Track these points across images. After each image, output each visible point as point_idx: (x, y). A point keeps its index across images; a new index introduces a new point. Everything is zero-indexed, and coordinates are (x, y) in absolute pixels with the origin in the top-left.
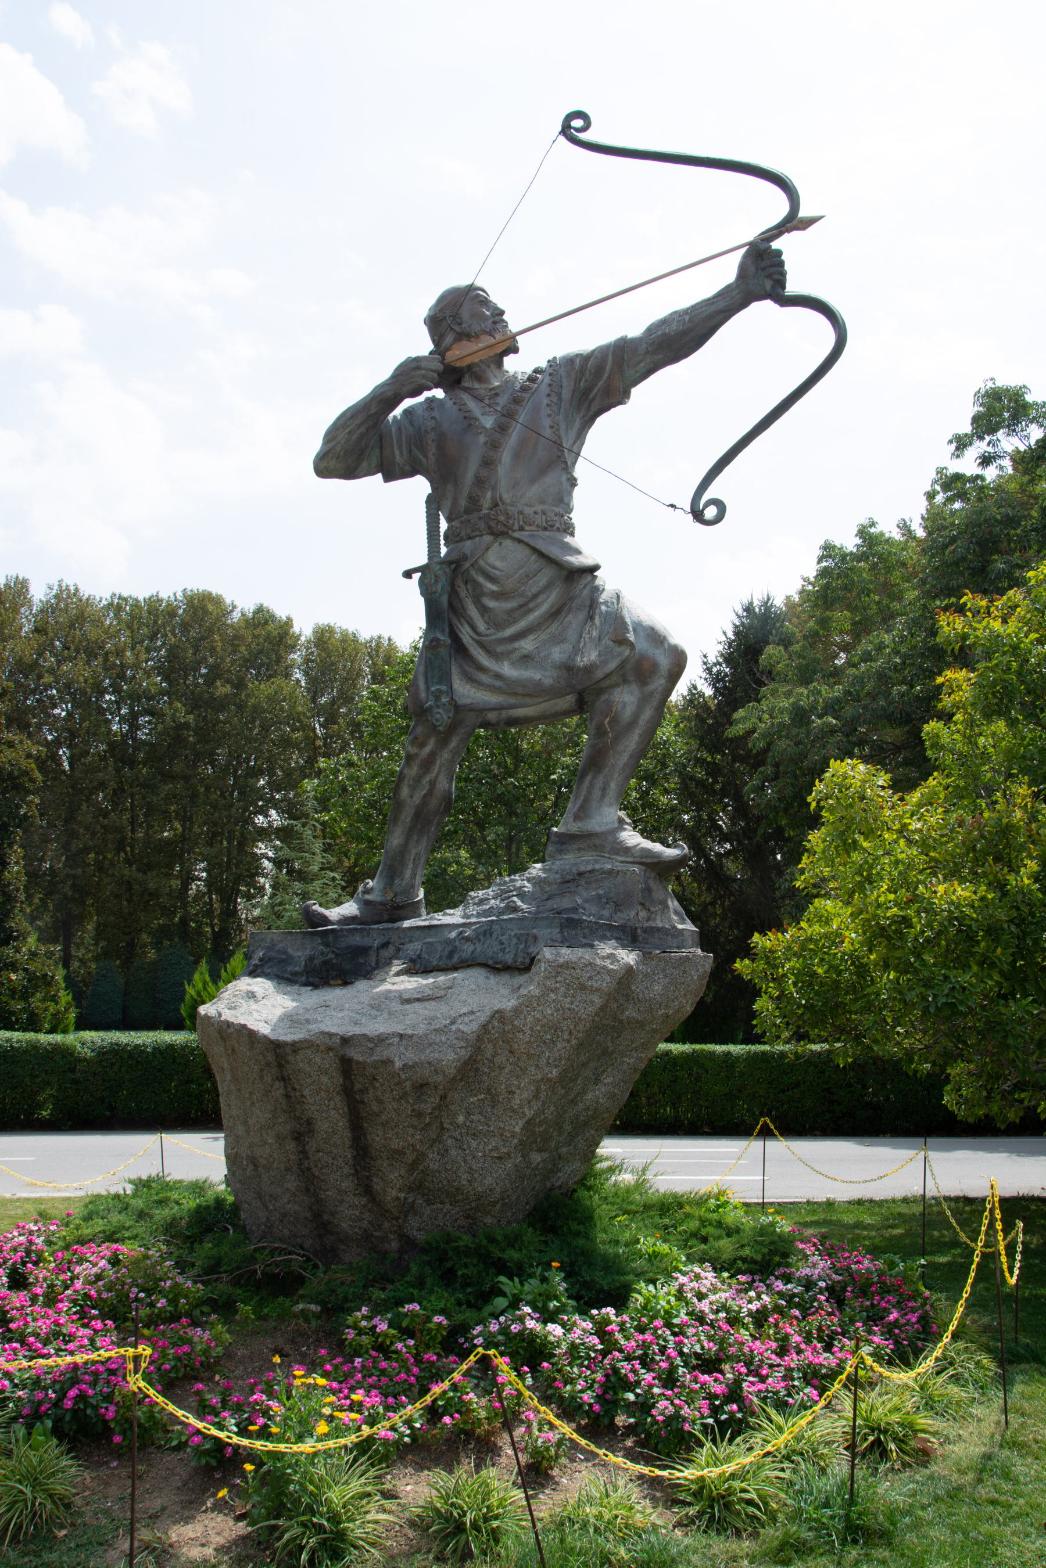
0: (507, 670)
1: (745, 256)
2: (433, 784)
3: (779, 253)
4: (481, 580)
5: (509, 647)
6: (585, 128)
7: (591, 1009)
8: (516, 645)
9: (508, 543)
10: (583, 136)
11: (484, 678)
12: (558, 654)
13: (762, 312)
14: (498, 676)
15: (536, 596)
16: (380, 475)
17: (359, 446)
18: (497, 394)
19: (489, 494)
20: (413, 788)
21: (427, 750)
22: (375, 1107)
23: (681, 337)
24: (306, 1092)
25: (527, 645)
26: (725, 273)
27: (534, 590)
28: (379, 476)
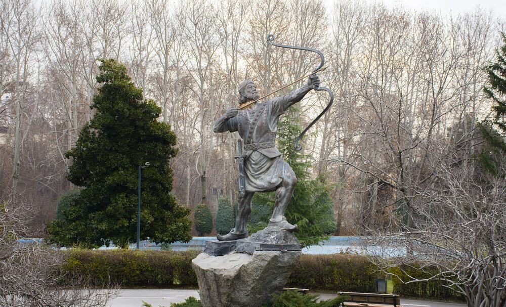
2: (245, 207)
7: (265, 265)
14: (255, 184)
15: (263, 164)
25: (263, 176)
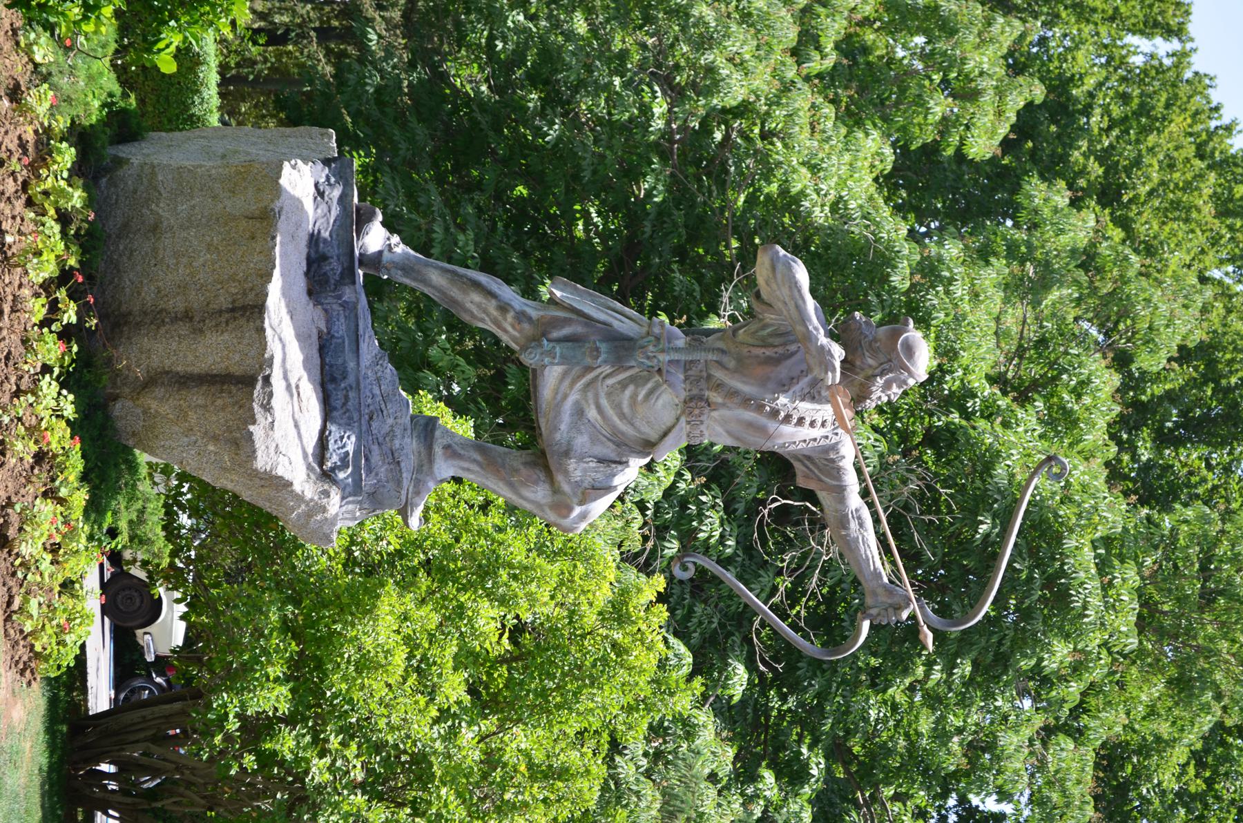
0: (574, 397)
2: (482, 320)
4: (649, 385)
5: (591, 401)
8: (593, 407)
11: (567, 383)
12: (581, 442)
14: (565, 396)
19: (720, 400)
20: (479, 306)
21: (510, 329)
22: (219, 402)
24: (226, 336)
25: (592, 413)
27: (638, 424)
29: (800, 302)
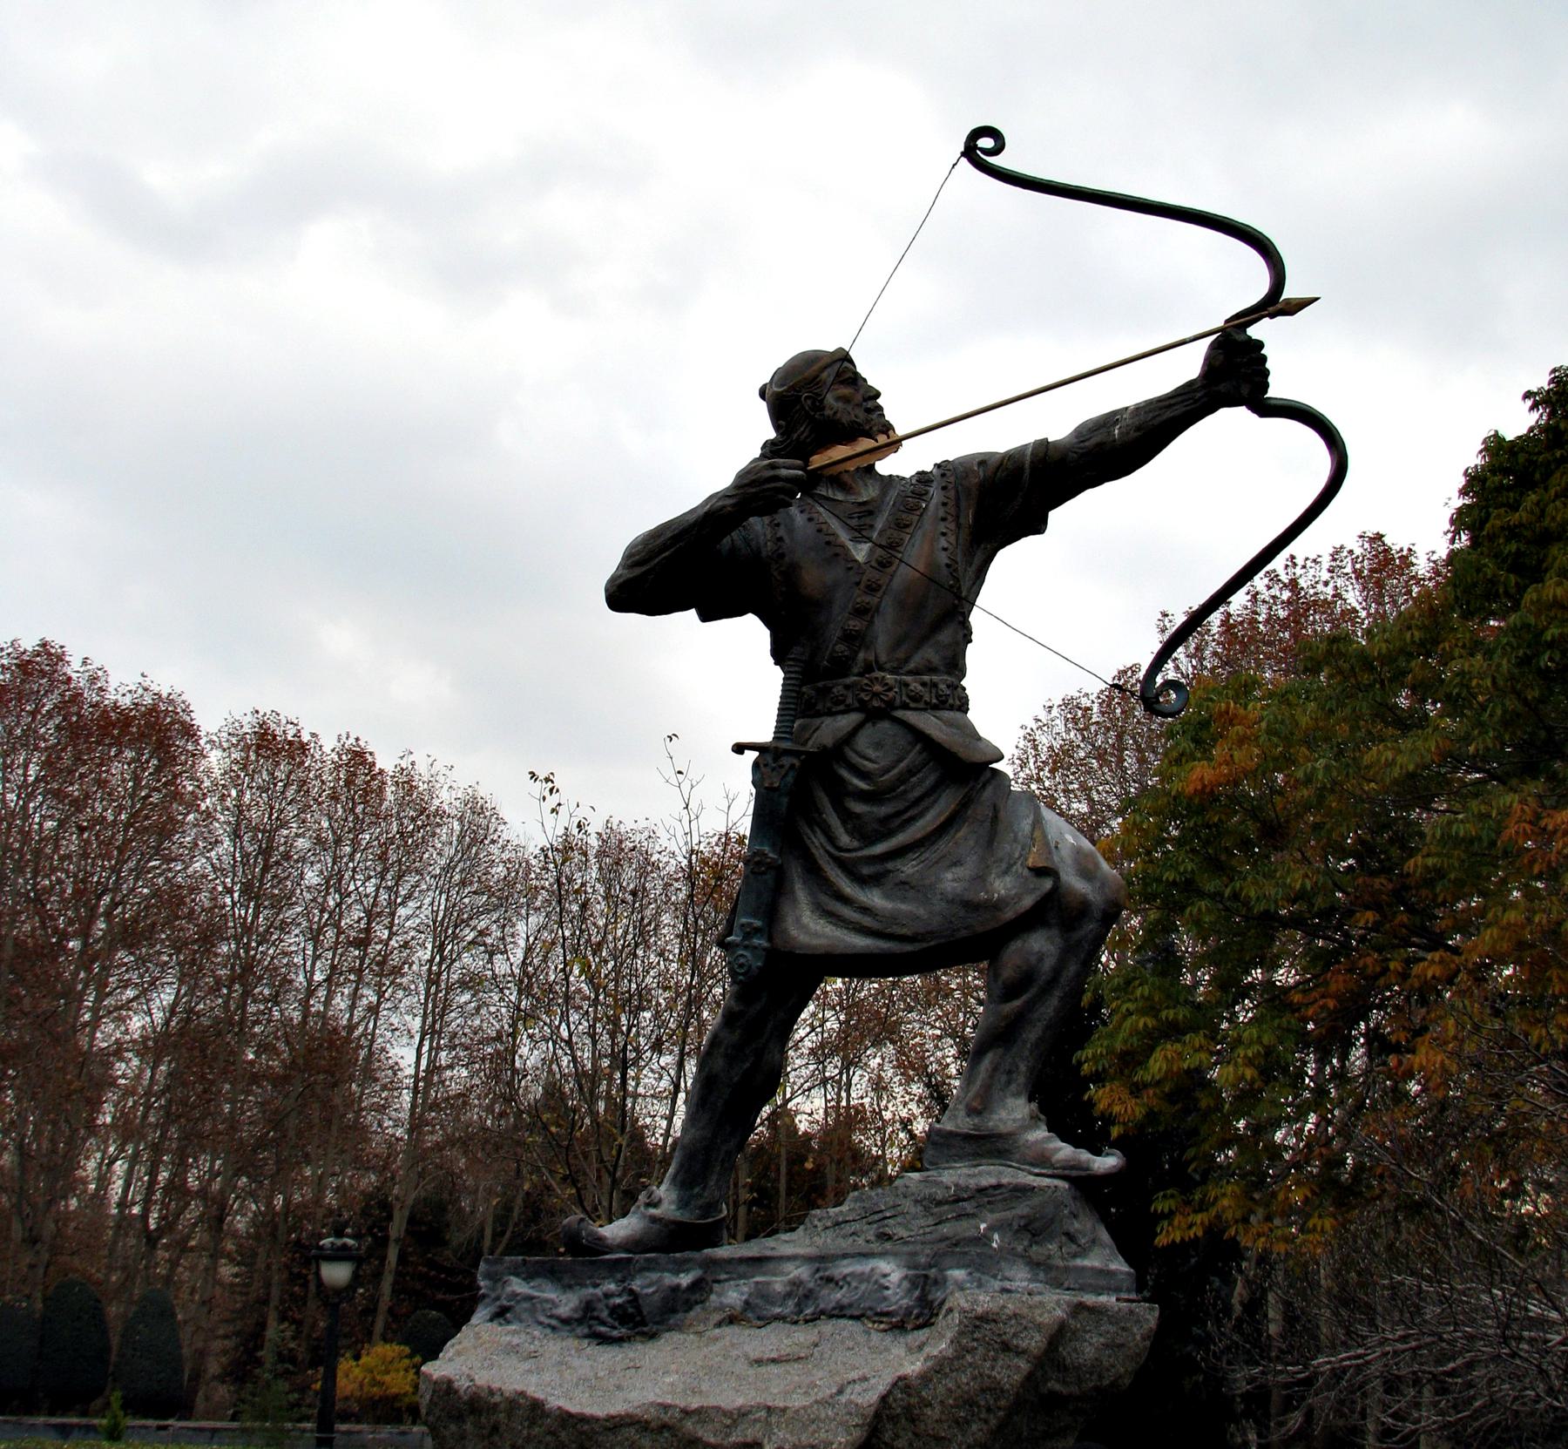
1: (1213, 346)
3: (1260, 345)
4: (845, 773)
6: (998, 149)
8: (890, 866)
9: (885, 725)
10: (992, 160)
12: (951, 881)
13: (1233, 420)
14: (865, 910)
16: (693, 612)
17: (673, 572)
18: (871, 513)
23: (1119, 447)
25: (908, 868)
26: (1188, 365)
27: (917, 793)
28: (692, 614)
29: (669, 534)
